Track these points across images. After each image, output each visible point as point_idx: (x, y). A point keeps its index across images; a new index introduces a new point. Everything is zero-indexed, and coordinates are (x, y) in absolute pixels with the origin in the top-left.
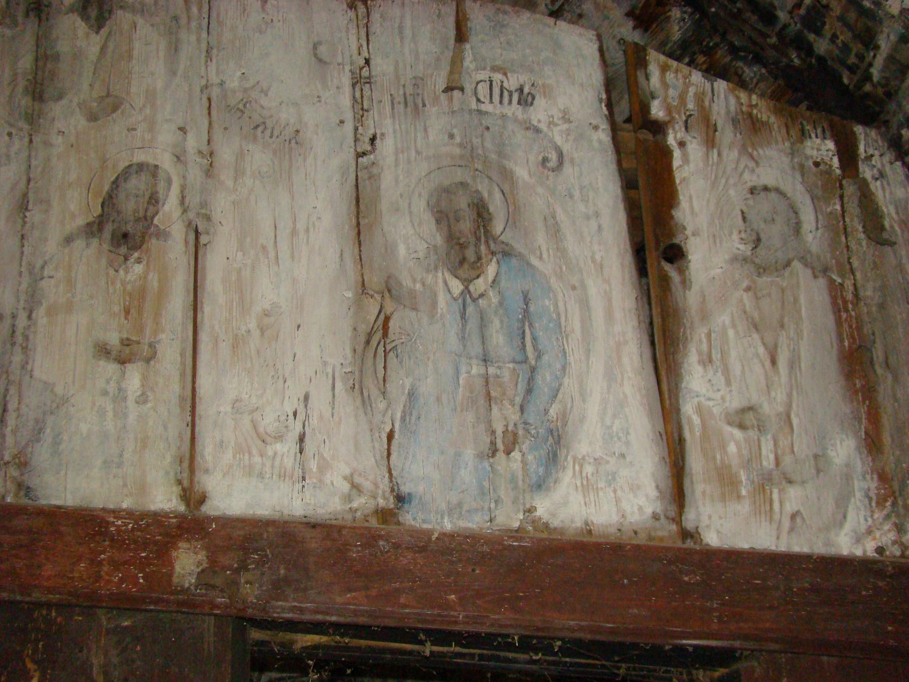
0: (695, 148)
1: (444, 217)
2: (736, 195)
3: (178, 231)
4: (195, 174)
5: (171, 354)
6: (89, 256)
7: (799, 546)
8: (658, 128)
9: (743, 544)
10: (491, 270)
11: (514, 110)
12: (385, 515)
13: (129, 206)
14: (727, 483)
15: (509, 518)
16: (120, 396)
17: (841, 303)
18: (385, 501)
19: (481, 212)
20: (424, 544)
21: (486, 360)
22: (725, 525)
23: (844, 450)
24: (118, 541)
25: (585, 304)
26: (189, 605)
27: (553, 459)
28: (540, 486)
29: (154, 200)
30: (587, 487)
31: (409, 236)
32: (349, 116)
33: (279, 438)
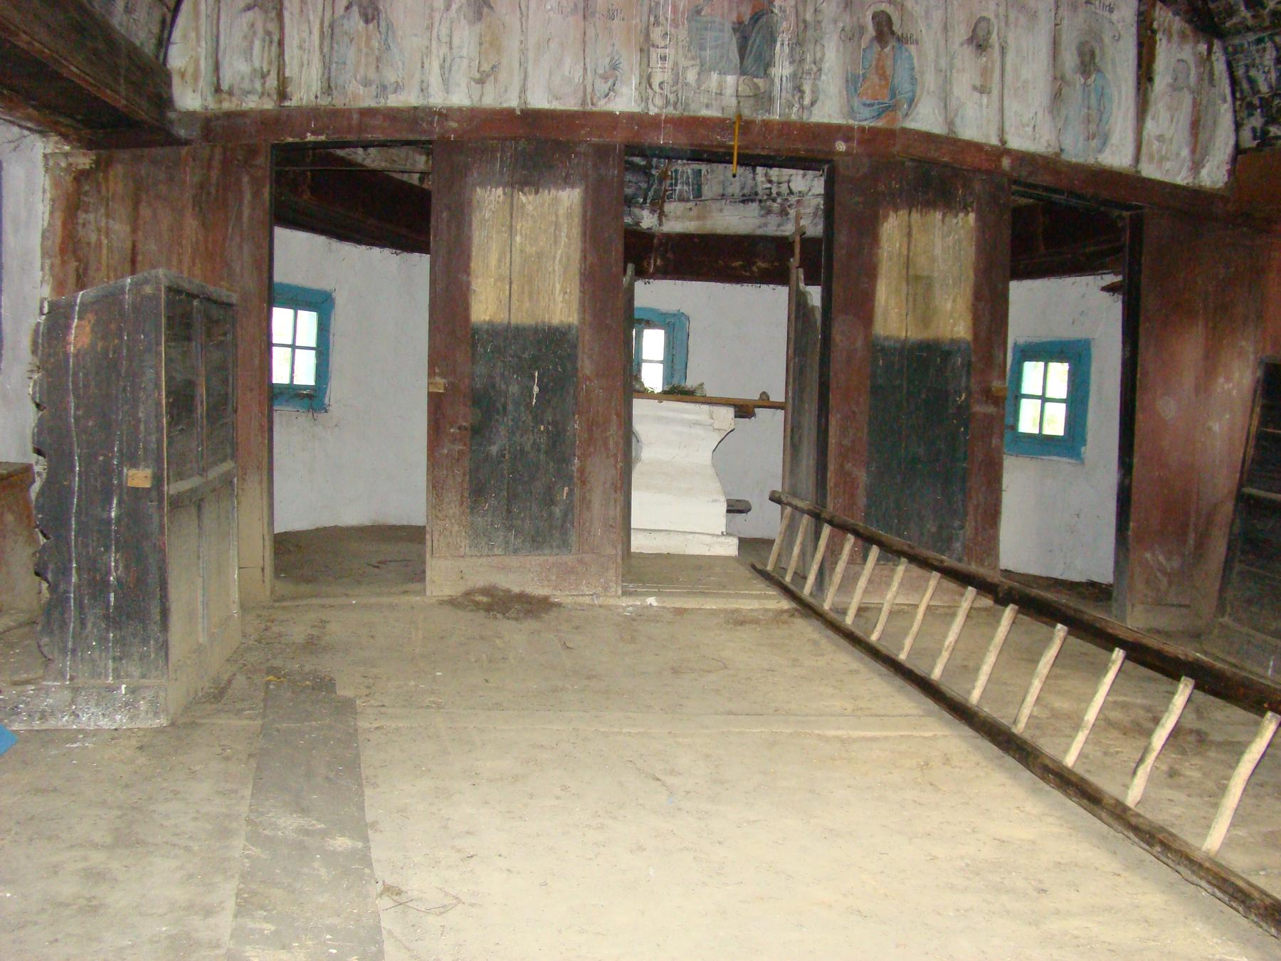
0: (1164, 42)
1: (1081, 54)
2: (1173, 61)
3: (997, 48)
4: (1003, 24)
5: (995, 92)
6: (968, 51)
7: (1167, 179)
8: (1154, 32)
9: (1153, 177)
10: (1093, 77)
11: (1106, 14)
12: (1057, 155)
13: (981, 33)
14: (1151, 158)
15: (1091, 161)
16: (981, 106)
17: (1196, 104)
18: (1057, 150)
19: (1093, 54)
20: (1070, 165)
22: (1149, 171)
23: (1185, 152)
24: (987, 153)
25: (1120, 92)
26: (1004, 174)
27: (1104, 144)
28: (1100, 151)
29: (989, 33)
30: (1113, 153)
31: (1070, 60)
32: (1053, 8)
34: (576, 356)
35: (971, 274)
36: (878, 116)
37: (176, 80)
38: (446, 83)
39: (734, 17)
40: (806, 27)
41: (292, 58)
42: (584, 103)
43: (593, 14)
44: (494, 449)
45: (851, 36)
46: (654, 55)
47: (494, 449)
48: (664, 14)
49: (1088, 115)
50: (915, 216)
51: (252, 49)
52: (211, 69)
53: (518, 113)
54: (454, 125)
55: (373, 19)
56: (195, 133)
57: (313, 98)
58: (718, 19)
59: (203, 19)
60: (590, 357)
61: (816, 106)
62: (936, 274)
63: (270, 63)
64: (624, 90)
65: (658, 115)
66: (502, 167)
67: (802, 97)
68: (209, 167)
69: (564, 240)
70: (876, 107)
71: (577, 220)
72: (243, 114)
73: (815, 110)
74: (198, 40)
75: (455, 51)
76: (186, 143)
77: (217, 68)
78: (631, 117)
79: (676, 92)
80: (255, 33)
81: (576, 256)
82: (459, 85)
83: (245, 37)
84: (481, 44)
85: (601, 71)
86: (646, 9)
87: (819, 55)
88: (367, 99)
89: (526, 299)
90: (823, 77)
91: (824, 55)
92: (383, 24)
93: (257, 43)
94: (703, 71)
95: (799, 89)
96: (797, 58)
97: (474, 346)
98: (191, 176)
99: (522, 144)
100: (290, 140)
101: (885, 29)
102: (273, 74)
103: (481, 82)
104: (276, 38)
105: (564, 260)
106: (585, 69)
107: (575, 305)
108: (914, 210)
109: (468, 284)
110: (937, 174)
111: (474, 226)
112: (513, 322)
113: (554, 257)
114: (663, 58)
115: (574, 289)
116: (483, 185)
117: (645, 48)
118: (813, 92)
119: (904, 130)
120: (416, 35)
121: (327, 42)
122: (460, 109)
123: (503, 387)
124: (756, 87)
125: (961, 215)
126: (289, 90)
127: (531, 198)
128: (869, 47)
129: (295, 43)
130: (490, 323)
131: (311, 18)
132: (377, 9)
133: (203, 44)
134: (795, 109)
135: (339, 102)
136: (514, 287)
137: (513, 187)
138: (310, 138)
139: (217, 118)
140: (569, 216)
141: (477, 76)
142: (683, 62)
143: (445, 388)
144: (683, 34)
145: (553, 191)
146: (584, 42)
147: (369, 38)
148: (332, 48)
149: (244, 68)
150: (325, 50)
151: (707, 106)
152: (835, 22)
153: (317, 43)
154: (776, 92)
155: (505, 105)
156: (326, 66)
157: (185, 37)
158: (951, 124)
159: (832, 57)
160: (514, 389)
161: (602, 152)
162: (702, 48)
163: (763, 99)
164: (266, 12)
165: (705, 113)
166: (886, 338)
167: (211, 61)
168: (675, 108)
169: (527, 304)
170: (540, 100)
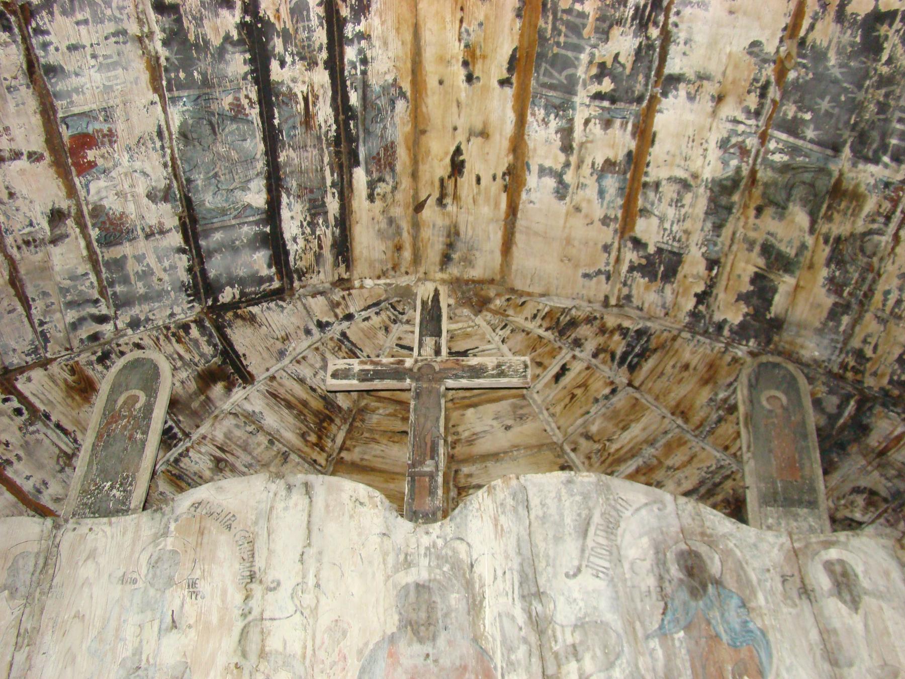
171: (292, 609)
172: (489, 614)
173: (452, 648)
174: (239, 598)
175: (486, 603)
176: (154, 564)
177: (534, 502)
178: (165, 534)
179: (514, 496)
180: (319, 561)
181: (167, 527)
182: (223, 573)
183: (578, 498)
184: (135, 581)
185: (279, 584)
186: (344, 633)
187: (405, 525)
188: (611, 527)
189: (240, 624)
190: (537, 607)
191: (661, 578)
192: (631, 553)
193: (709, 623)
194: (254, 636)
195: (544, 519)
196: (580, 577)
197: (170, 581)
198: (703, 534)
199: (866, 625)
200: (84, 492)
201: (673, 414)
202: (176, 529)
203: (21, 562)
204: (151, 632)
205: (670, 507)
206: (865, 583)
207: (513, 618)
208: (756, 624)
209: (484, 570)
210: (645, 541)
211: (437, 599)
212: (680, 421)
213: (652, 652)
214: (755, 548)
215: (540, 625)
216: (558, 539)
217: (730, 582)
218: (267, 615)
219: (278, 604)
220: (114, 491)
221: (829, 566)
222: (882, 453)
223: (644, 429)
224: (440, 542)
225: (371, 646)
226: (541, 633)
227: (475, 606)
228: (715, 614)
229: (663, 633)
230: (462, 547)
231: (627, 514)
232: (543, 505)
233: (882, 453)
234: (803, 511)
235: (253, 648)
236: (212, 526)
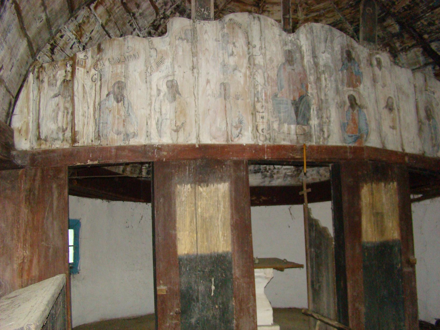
3: (396, 109)
4: (397, 100)
6: (386, 111)
10: (431, 120)
11: (432, 95)
12: (423, 154)
13: (390, 104)
15: (435, 156)
20: (428, 158)
21: (432, 134)
29: (393, 103)
31: (423, 114)
32: (414, 92)
33: (411, 142)
34: (231, 268)
35: (397, 209)
36: (355, 142)
37: (16, 134)
38: (160, 132)
39: (292, 98)
40: (322, 102)
41: (79, 121)
42: (227, 140)
43: (229, 97)
44: (193, 321)
45: (341, 105)
46: (258, 117)
47: (193, 321)
48: (262, 96)
49: (432, 137)
50: (374, 185)
51: (57, 116)
52: (35, 127)
53: (197, 146)
54: (165, 153)
55: (121, 101)
56: (27, 162)
57: (90, 141)
58: (285, 99)
59: (31, 102)
60: (238, 267)
61: (331, 137)
62: (384, 211)
63: (67, 124)
64: (246, 133)
65: (263, 145)
66: (189, 174)
67: (323, 134)
68: (34, 180)
69: (222, 209)
70: (354, 137)
71: (228, 199)
72: (53, 151)
73: (330, 140)
74: (29, 113)
75: (163, 116)
76: (22, 167)
77: (39, 127)
78: (251, 147)
79: (269, 134)
80: (59, 109)
81: (229, 217)
82: (166, 133)
83: (54, 111)
84: (176, 112)
85: (234, 124)
86: (253, 95)
87: (328, 115)
88: (119, 142)
89: (205, 241)
90: (331, 125)
91: (330, 114)
92: (126, 102)
93: (60, 114)
94: (281, 123)
95: (322, 130)
96: (320, 116)
97: (180, 268)
98: (24, 186)
99: (199, 162)
100: (79, 164)
101: (354, 102)
102: (69, 130)
103: (177, 131)
104: (70, 111)
105: (223, 219)
106: (227, 124)
107: (230, 242)
108: (373, 183)
109: (176, 235)
110: (382, 165)
111: (177, 205)
112: (199, 253)
113: (218, 218)
114: (262, 118)
115: (228, 233)
116: (180, 183)
117: (254, 113)
118: (328, 131)
119: (367, 147)
120: (143, 108)
121: (97, 113)
122: (168, 146)
123: (196, 288)
124: (304, 130)
125: (391, 183)
126: (77, 137)
127: (205, 189)
128: (348, 110)
129: (81, 113)
130: (188, 254)
131: (89, 100)
132: (122, 95)
133: (31, 114)
134: (321, 140)
135: (104, 143)
136: (199, 235)
137: (195, 184)
138: (89, 162)
139: (39, 153)
140: (224, 197)
141: (175, 128)
142: (272, 119)
143: (167, 292)
144: (270, 106)
145: (216, 185)
146: (226, 110)
147: (119, 111)
148: (100, 116)
149: (53, 127)
150: (97, 117)
151: (284, 140)
152: (333, 99)
153: (92, 113)
154: (313, 132)
155: (190, 143)
156: (97, 124)
157: (21, 111)
158: (383, 143)
159: (334, 115)
160: (201, 288)
161: (237, 164)
162: (279, 112)
163: (307, 135)
164: (65, 98)
165: (283, 143)
166: (368, 243)
167: (35, 124)
168: (270, 141)
169: (206, 243)
170: (206, 140)
171: (259, 53)
172: (305, 60)
173: (297, 68)
174: (246, 49)
175: (305, 57)
176: (223, 36)
177: (315, 31)
178: (224, 28)
179: (310, 28)
180: (265, 40)
181: (224, 26)
182: (241, 41)
183: (325, 32)
184: (219, 41)
185: (256, 46)
186: (273, 61)
187: (284, 34)
188: (332, 42)
189: (248, 56)
190: (316, 60)
191: (342, 56)
192: (336, 49)
193: (351, 69)
194: (252, 59)
195: (317, 36)
196: (325, 54)
197: (228, 42)
198: (351, 46)
199: (382, 75)
200: (197, 11)
201: (334, 3)
202: (227, 26)
203: (187, 32)
204: (226, 56)
205: (345, 38)
206: (383, 64)
207: (311, 62)
208: (360, 71)
209: (304, 48)
210: (339, 46)
211: (293, 54)
212: (335, 6)
213: (339, 74)
214: (362, 51)
215: (316, 65)
216: (320, 43)
217: (356, 60)
218: (254, 54)
219: (256, 51)
220: (205, 12)
221: (377, 59)
222: (386, 27)
223: (324, 5)
224: (293, 39)
225: (279, 65)
226: (316, 66)
227: (302, 58)
228: (353, 67)
229: (342, 70)
230: (298, 41)
231: (336, 38)
232: (316, 32)
233: (386, 27)
234: (372, 44)
235: (252, 63)
236: (236, 28)
